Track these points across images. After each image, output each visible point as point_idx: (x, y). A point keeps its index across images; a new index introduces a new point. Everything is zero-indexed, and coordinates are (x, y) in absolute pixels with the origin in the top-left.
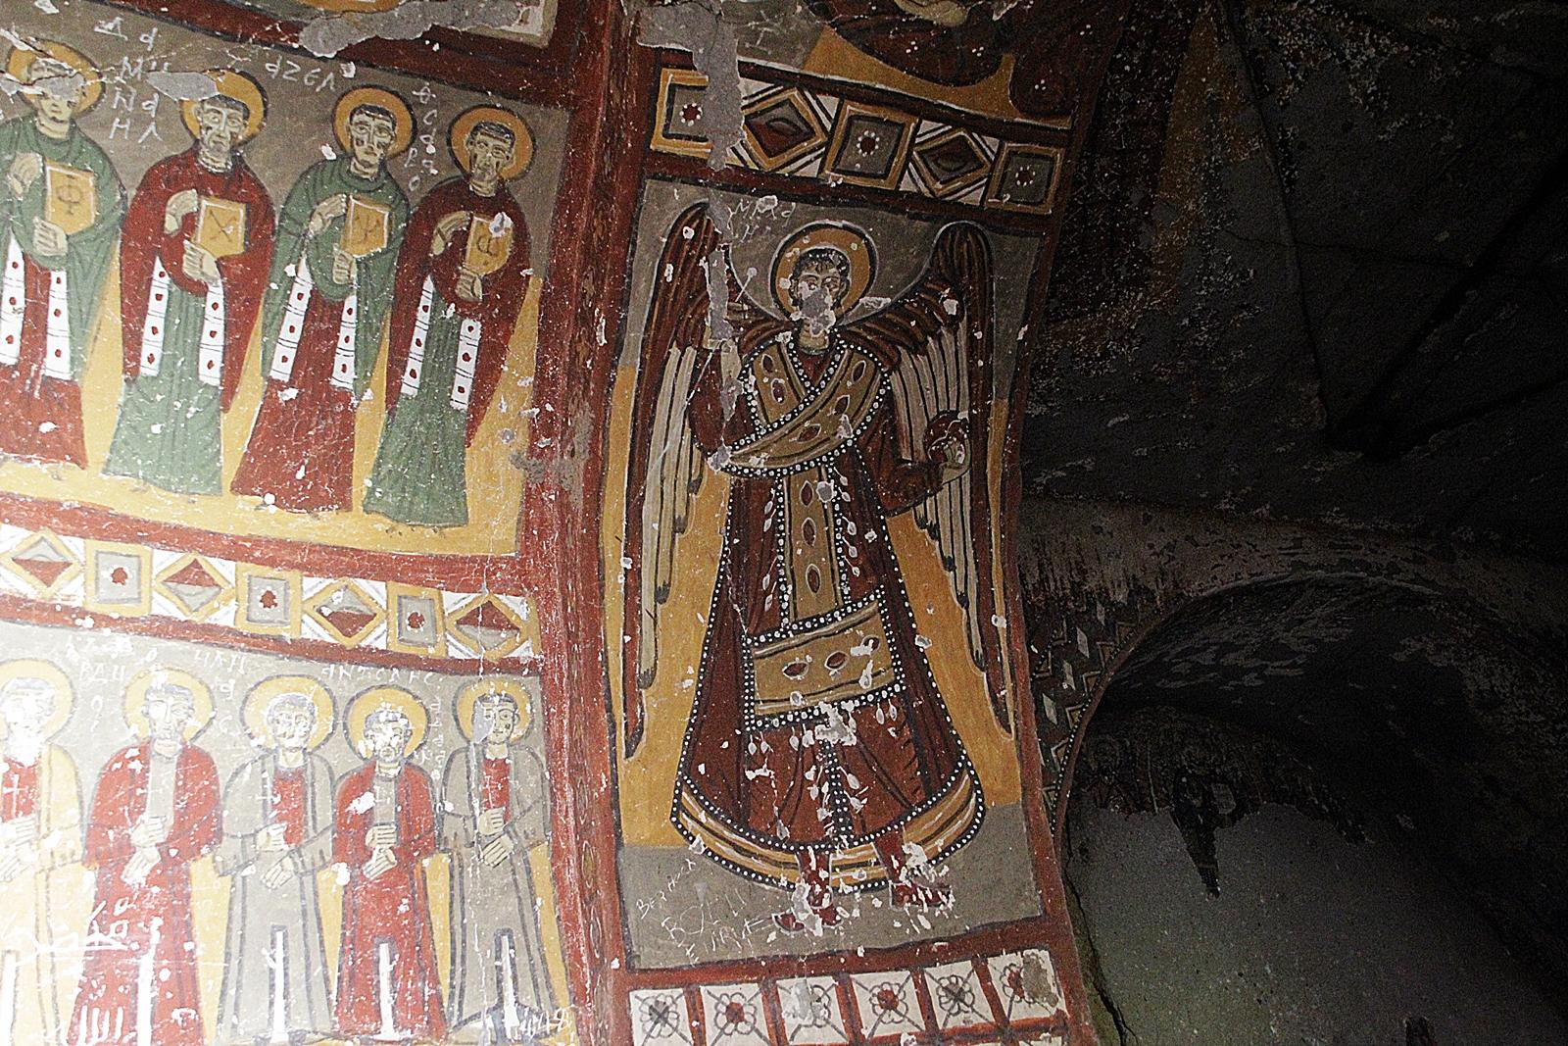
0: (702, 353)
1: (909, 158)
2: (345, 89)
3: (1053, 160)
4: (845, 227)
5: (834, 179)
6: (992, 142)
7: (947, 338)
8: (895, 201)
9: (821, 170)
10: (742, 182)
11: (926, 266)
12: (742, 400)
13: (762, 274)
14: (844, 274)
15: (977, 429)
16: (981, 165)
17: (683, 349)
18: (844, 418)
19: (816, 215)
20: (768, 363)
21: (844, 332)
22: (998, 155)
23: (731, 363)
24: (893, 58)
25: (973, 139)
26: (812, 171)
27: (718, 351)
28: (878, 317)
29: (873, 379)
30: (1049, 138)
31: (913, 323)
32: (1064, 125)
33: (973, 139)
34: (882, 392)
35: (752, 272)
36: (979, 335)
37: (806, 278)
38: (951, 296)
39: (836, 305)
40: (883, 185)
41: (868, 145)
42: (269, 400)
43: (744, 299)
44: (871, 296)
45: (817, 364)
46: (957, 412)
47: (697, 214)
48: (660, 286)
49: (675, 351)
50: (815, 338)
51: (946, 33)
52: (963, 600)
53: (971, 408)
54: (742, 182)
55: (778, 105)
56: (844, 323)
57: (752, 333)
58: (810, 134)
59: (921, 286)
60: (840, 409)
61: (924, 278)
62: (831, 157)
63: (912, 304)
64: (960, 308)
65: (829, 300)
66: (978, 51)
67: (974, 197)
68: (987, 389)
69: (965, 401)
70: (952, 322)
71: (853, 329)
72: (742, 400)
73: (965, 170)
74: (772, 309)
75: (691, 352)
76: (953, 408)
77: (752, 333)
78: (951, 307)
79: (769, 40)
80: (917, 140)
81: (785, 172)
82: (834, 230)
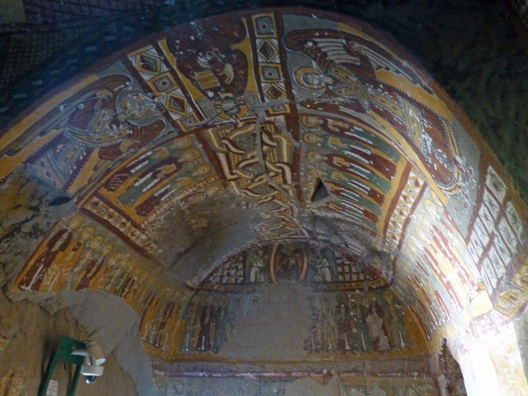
0: (339, 105)
1: (270, 63)
2: (304, 141)
3: (256, 19)
4: (295, 75)
5: (283, 79)
6: (258, 41)
7: (320, 45)
8: (283, 63)
9: (281, 82)
10: (290, 96)
11: (299, 52)
12: (350, 99)
13: (314, 92)
14: (309, 74)
15: (349, 37)
16: (265, 42)
17: (339, 108)
18: (350, 78)
19: (294, 82)
20: (340, 92)
21: (326, 73)
22: (260, 38)
23: (341, 99)
24: (246, 75)
25: (259, 47)
26: (283, 85)
27: (339, 102)
28: (319, 64)
29: (337, 67)
30: (250, 23)
31: (318, 55)
32: (244, 20)
33: (259, 47)
34: (341, 65)
35: (314, 94)
36: (317, 34)
37: (312, 82)
38: (306, 44)
39: (318, 75)
40: (280, 67)
41: (270, 74)
42: (372, 166)
43: (323, 95)
44: (312, 65)
45: (336, 81)
46: (343, 44)
47: (302, 104)
48: (324, 110)
49: (341, 110)
50: (330, 81)
51: (234, 66)
52: (398, 72)
53: (341, 38)
54: (290, 96)
55: (268, 94)
56: (322, 72)
57: (331, 94)
58: (273, 87)
59: (306, 54)
60: (348, 78)
61: (304, 52)
62: (277, 81)
63: (313, 55)
64: (310, 41)
65: (318, 76)
66: (234, 56)
67: (275, 42)
68: (335, 31)
69: (339, 40)
70: (315, 43)
71: (324, 70)
72: (350, 99)
73: (268, 46)
74: (324, 90)
75: (340, 107)
76: (342, 45)
77: (331, 94)
78: (310, 44)
79: (254, 99)
80: (265, 61)
81: (285, 90)
82: (297, 78)
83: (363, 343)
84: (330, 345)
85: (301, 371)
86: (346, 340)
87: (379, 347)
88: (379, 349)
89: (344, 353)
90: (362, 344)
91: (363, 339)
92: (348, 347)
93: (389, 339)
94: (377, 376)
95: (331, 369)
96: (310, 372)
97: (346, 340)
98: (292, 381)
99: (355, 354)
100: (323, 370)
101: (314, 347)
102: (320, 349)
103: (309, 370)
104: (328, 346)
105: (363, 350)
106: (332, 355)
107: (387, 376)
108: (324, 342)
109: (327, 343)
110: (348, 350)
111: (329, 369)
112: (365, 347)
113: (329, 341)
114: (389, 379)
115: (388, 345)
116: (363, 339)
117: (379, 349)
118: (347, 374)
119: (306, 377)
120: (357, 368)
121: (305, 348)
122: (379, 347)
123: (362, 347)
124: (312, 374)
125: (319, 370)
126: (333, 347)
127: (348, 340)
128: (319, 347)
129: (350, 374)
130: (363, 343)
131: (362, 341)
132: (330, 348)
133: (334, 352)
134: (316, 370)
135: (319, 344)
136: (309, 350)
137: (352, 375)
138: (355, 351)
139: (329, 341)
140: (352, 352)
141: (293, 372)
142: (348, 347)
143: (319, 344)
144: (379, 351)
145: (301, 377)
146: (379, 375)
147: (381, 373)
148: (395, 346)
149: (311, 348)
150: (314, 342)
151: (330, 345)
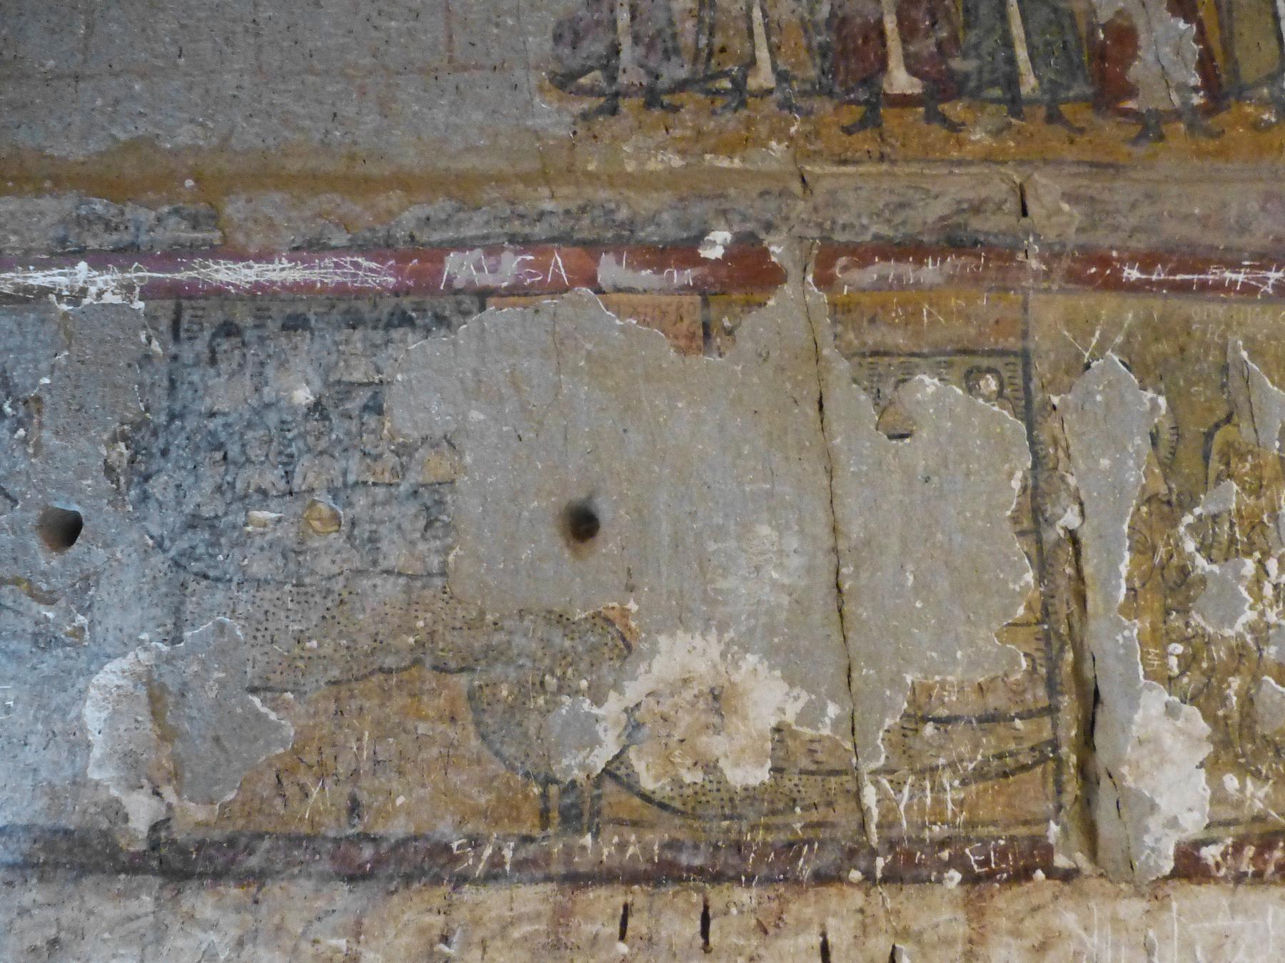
83: (1022, 53)
84: (763, 54)
85: (523, 243)
86: (890, 24)
87: (1131, 92)
88: (1130, 104)
89: (870, 120)
90: (1011, 60)
91: (1017, 30)
92: (900, 80)
93: (1201, 37)
94: (1115, 284)
95: (769, 227)
96: (593, 247)
97: (890, 24)
98: (441, 320)
99: (954, 127)
100: (699, 238)
101: (630, 74)
102: (681, 86)
103: (584, 230)
104: (752, 63)
105: (1015, 104)
106: (779, 133)
107: (1184, 288)
108: (719, 41)
109: (738, 45)
110: (904, 101)
111: (750, 226)
112: (1029, 84)
113: (759, 30)
114: (1199, 311)
115: (1195, 80)
116: (1017, 30)
117: (1130, 104)
118: (891, 269)
119: (558, 289)
120: (976, 223)
121: (565, 81)
122: (1131, 92)
123: (1012, 81)
124: (609, 270)
125: (673, 233)
126: (782, 77)
127: (908, 31)
128: (676, 71)
129: (908, 270)
130: (1022, 53)
131: (1008, 43)
132: (763, 77)
133: (786, 105)
134: (649, 234)
135: (677, 51)
136: (591, 92)
137: (931, 272)
138: (956, 110)
139: (759, 30)
140: (934, 116)
141: (460, 245)
142: (900, 80)
143: (677, 51)
144: (1127, 113)
145: (516, 291)
146: (1133, 274)
147: (1147, 261)
148: (1241, 93)
149: (612, 79)
150: (636, 39)
151: (763, 54)
